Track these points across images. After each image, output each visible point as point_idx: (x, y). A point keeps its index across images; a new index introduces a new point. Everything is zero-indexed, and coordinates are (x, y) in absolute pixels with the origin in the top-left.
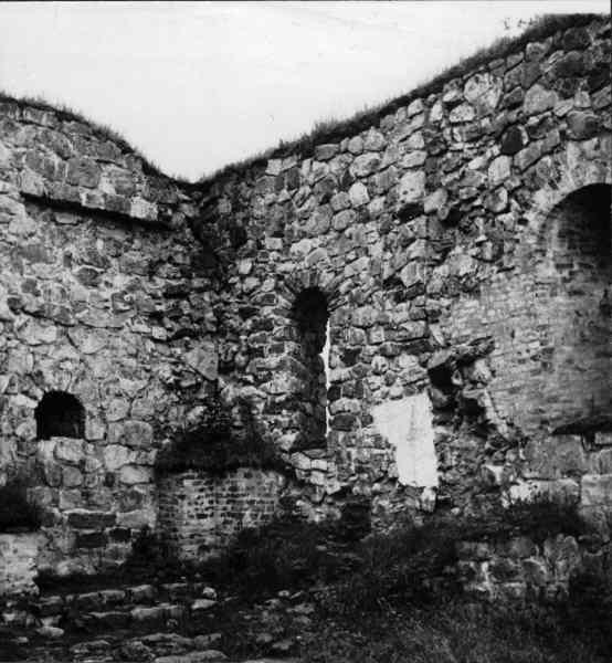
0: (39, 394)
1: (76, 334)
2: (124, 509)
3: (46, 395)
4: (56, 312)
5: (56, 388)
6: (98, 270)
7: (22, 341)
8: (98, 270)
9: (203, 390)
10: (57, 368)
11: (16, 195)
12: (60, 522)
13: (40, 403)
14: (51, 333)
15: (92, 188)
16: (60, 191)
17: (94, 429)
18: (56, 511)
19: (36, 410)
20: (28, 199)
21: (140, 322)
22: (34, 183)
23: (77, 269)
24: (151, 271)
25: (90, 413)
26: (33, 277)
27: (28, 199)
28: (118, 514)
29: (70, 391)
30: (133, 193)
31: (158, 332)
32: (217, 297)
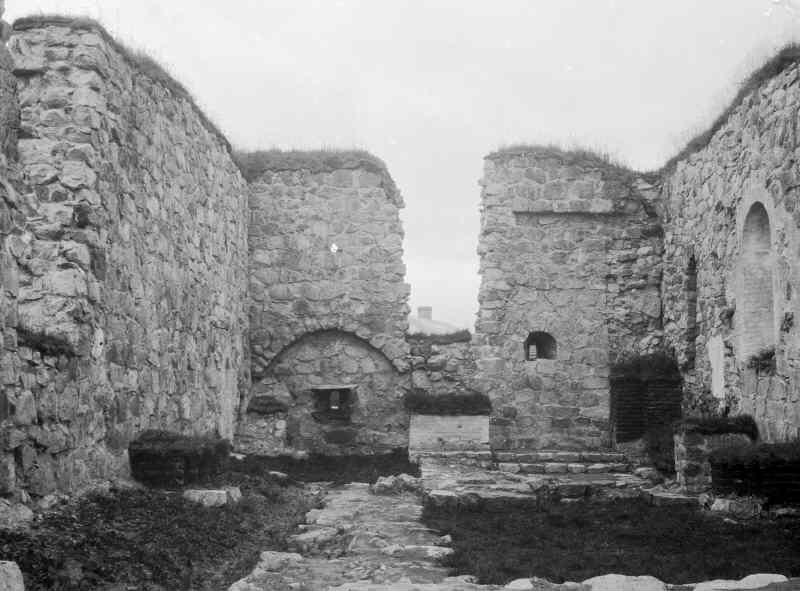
0: (527, 334)
1: (552, 296)
2: (585, 405)
3: (531, 334)
4: (538, 282)
5: (537, 330)
6: (567, 252)
7: (515, 302)
8: (567, 252)
9: (650, 325)
10: (536, 317)
11: (510, 213)
12: (541, 411)
13: (528, 340)
14: (533, 296)
15: (561, 199)
16: (537, 206)
17: (561, 353)
18: (538, 404)
19: (524, 343)
20: (517, 214)
21: (597, 283)
22: (521, 204)
23: (551, 253)
24: (608, 247)
25: (561, 345)
26: (522, 262)
27: (517, 214)
28: (581, 408)
29: (546, 331)
30: (592, 196)
31: (613, 288)
32: (659, 259)
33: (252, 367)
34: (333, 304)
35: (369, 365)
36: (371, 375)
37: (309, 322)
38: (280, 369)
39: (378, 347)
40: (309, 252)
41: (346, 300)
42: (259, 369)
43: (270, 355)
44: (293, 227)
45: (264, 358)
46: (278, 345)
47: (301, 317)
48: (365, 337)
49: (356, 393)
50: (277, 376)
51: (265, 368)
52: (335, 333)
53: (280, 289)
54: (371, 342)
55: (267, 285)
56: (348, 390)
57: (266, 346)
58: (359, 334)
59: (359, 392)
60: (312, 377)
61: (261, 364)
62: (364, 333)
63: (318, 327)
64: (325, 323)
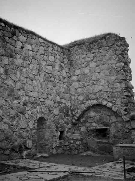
33: (72, 120)
34: (98, 95)
35: (114, 119)
36: (115, 122)
37: (90, 102)
38: (83, 120)
39: (115, 111)
40: (89, 74)
41: (102, 92)
42: (74, 121)
43: (78, 115)
44: (83, 66)
45: (75, 116)
46: (80, 112)
47: (88, 100)
48: (110, 107)
49: (109, 130)
50: (82, 123)
51: (77, 120)
52: (99, 105)
53: (79, 90)
54: (112, 109)
55: (76, 89)
56: (106, 129)
57: (76, 112)
58: (107, 106)
59: (110, 130)
60: (94, 124)
61: (75, 119)
62: (110, 105)
63: (93, 104)
64: (95, 102)
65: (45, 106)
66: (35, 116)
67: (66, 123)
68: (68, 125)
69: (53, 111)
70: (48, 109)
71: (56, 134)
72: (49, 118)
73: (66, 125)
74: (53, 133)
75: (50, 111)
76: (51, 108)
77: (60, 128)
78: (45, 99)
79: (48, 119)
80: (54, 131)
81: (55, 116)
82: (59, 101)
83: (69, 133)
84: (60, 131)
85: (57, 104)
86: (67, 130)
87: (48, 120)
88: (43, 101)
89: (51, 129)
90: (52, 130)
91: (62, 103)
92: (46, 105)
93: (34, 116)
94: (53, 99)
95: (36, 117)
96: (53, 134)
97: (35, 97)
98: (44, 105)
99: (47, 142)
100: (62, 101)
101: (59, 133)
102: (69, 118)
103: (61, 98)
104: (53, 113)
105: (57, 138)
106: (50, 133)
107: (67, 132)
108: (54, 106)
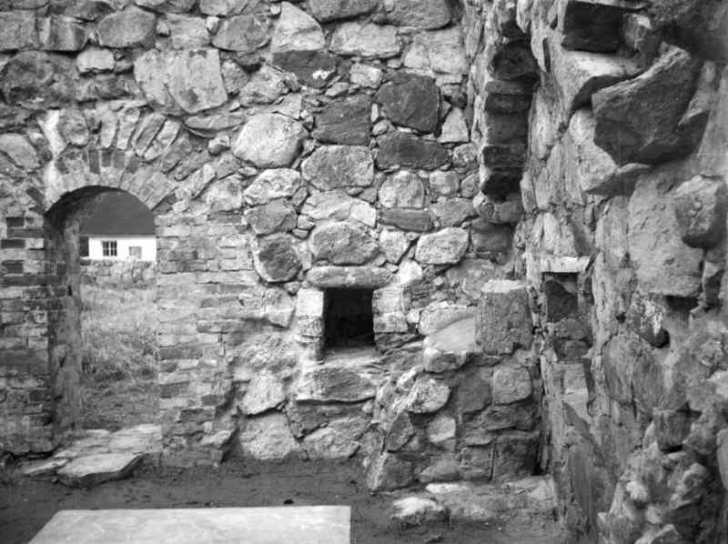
65: (129, 104)
66: (24, 186)
67: (388, 219)
68: (424, 239)
69: (232, 130)
70: (171, 128)
71: (280, 312)
72: (188, 187)
73: (396, 235)
74: (237, 306)
75: (199, 137)
76: (205, 113)
77: (316, 261)
78: (127, 52)
79: (169, 200)
80: (244, 287)
81: (247, 171)
82: (314, 42)
83: (433, 305)
84: (331, 282)
85: (270, 80)
86: (409, 273)
87: (178, 207)
88: (106, 72)
89: (206, 277)
90: (220, 277)
91: (347, 56)
92: (144, 95)
93: (13, 190)
94: (221, 41)
95: (34, 193)
96: (245, 311)
97: (14, 46)
98: (126, 95)
99: (171, 369)
100: (347, 48)
101: (311, 304)
102: (438, 177)
103: (330, 24)
104: (225, 149)
105: (293, 336)
106: (205, 303)
107: (418, 294)
108: (233, 96)
